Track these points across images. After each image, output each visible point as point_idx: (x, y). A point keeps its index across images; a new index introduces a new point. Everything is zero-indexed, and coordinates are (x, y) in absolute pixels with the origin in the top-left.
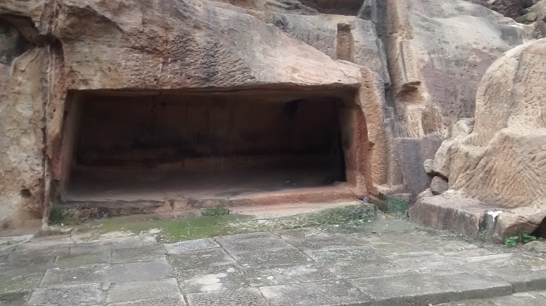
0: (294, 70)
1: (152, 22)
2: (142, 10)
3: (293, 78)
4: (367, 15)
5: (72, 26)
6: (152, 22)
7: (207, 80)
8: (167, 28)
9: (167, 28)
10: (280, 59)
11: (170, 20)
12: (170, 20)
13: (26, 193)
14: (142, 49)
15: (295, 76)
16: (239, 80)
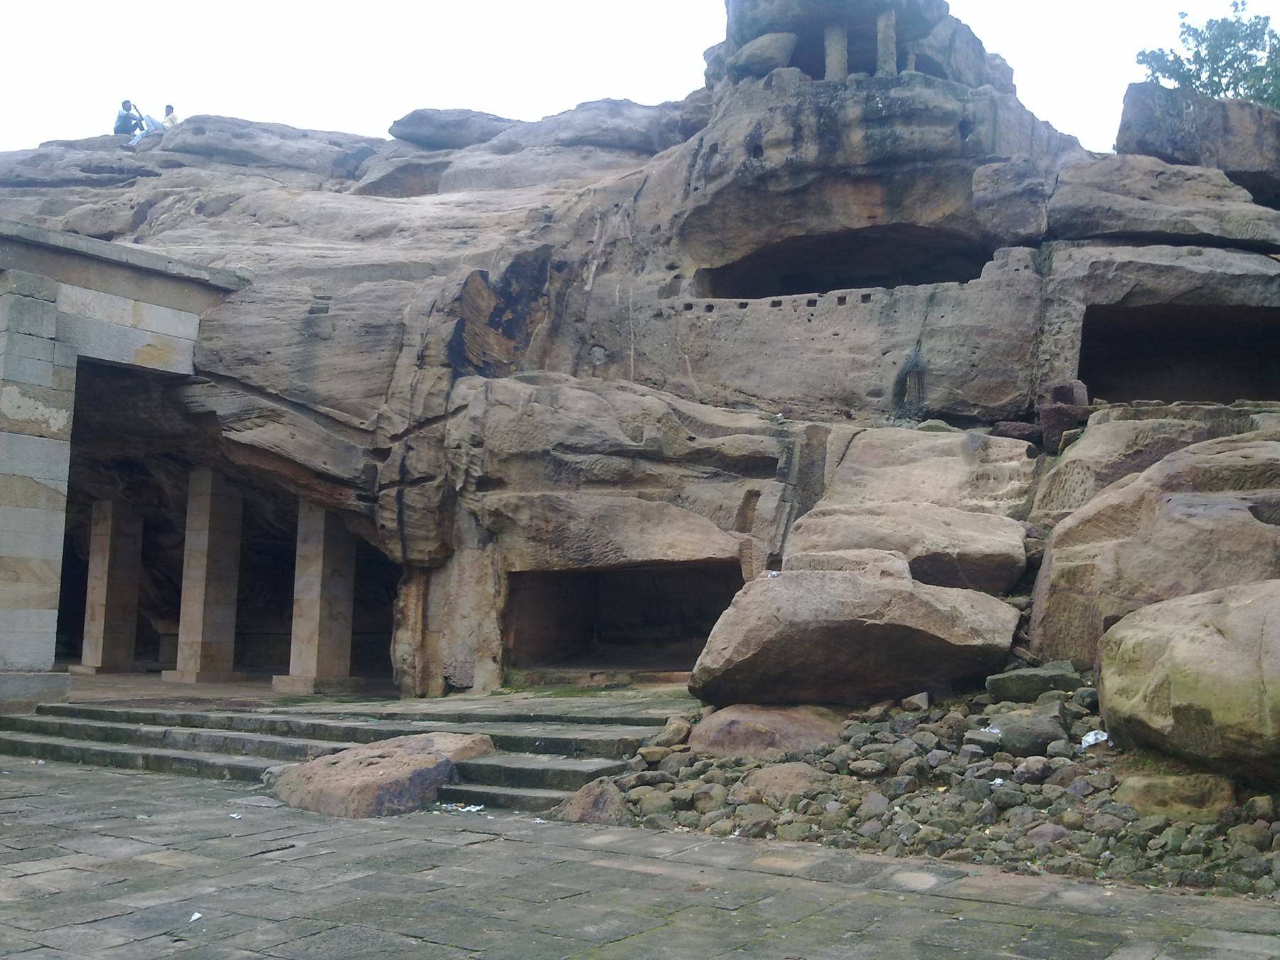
0: (671, 546)
1: (537, 517)
2: (530, 509)
3: (665, 554)
4: (783, 477)
5: (493, 523)
6: (537, 517)
7: (585, 561)
8: (547, 521)
9: (547, 521)
10: (659, 537)
11: (549, 514)
12: (549, 514)
13: (494, 659)
14: (534, 539)
15: (669, 552)
16: (612, 559)
